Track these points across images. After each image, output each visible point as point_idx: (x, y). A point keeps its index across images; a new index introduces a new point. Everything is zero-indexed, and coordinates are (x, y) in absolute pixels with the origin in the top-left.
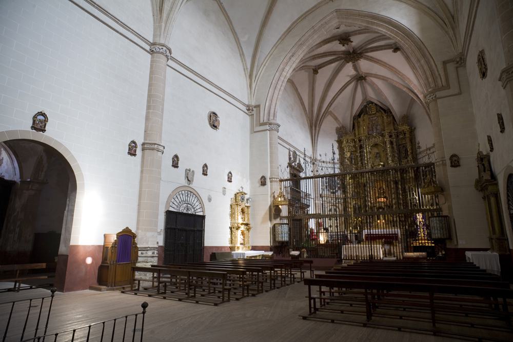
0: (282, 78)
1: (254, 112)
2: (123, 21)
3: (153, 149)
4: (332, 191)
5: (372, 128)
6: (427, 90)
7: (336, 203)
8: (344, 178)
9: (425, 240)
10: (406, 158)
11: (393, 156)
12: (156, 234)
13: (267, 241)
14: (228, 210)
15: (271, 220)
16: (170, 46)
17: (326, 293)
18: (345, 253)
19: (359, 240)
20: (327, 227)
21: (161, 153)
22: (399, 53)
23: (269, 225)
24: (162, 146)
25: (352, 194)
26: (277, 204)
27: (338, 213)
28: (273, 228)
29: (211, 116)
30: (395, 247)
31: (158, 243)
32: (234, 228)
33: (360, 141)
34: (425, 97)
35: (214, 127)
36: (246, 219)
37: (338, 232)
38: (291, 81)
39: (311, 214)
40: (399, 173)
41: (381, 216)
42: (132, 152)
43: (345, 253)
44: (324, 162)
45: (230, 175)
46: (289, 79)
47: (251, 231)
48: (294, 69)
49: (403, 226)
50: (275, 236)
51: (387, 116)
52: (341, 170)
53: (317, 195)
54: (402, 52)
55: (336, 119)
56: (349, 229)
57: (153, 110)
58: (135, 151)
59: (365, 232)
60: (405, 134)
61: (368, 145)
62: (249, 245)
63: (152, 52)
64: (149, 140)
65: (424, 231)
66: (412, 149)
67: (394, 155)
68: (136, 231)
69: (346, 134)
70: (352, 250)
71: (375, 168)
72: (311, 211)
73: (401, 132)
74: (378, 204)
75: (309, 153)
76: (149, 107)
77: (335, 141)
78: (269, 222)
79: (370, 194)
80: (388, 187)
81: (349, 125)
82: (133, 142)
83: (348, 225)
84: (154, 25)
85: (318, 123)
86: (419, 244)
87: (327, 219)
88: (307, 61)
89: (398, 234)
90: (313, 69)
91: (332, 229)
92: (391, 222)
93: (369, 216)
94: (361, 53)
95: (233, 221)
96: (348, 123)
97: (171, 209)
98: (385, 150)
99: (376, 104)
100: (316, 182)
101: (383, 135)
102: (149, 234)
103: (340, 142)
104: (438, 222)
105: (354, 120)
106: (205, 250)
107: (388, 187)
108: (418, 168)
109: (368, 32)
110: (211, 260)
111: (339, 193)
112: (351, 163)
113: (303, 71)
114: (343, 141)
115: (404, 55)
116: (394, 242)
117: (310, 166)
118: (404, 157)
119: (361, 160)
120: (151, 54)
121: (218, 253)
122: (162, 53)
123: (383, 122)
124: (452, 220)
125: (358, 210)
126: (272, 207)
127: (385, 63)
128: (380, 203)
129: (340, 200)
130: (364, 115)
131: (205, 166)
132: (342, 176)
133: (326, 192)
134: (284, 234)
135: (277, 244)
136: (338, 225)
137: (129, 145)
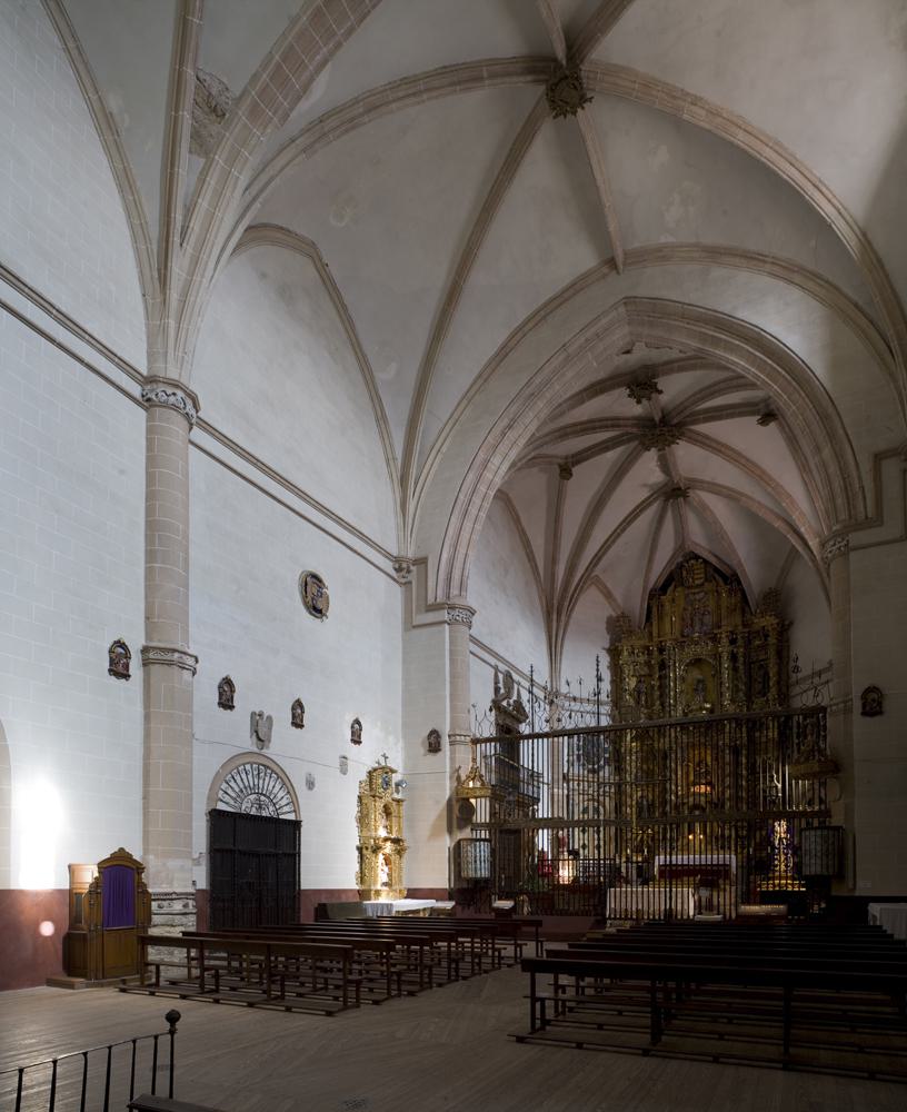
0: (482, 488)
1: (413, 577)
2: (63, 309)
3: (170, 663)
4: (590, 767)
5: (692, 620)
6: (830, 528)
7: (598, 795)
8: (620, 737)
9: (787, 878)
10: (764, 696)
11: (735, 689)
12: (190, 862)
13: (440, 878)
14: (354, 809)
15: (450, 831)
16: (194, 387)
17: (568, 989)
18: (613, 906)
19: (645, 877)
20: (576, 847)
21: (190, 673)
22: (773, 425)
23: (447, 842)
24: (191, 656)
25: (636, 776)
26: (465, 796)
27: (602, 818)
28: (454, 848)
29: (306, 584)
30: (722, 894)
31: (194, 883)
32: (367, 848)
33: (661, 651)
34: (823, 545)
35: (317, 610)
36: (395, 829)
37: (599, 859)
38: (503, 497)
39: (543, 819)
40: (744, 729)
41: (697, 825)
42: (119, 668)
43: (613, 906)
44: (575, 699)
45: (356, 726)
46: (499, 490)
47: (406, 855)
48: (513, 465)
49: (743, 848)
50: (459, 864)
51: (730, 592)
52: (613, 719)
53: (556, 777)
54: (780, 424)
55: (608, 595)
56: (624, 853)
57: (163, 562)
58: (127, 667)
59: (660, 860)
60: (766, 636)
61: (680, 661)
62: (402, 887)
63: (147, 403)
64: (159, 641)
65: (786, 859)
66: (779, 673)
67: (737, 686)
68: (143, 859)
69: (631, 632)
70: (629, 899)
71: (690, 716)
72: (543, 811)
73: (758, 632)
74: (691, 799)
75: (542, 677)
76: (150, 556)
78: (447, 837)
79: (676, 775)
80: (717, 759)
81: (637, 612)
82: (120, 644)
83: (624, 844)
84: (147, 325)
85: (566, 604)
86: (774, 886)
87: (576, 829)
88: (546, 443)
89: (730, 866)
90: (560, 466)
91: (586, 851)
92: (717, 838)
93: (671, 825)
94: (680, 425)
95: (364, 834)
96: (636, 606)
97: (221, 806)
98: (718, 673)
99: (705, 561)
100: (556, 745)
101: (715, 639)
102: (173, 864)
103: (614, 652)
104: (818, 840)
105: (649, 599)
106: (302, 898)
107: (717, 759)
108: (789, 718)
109: (703, 367)
110: (316, 920)
111: (606, 773)
112: (638, 702)
113: (535, 470)
114: (622, 650)
115: (785, 432)
116: (721, 881)
117: (542, 709)
118: (759, 693)
119: (661, 696)
120: (146, 409)
121: (333, 905)
122: (175, 407)
123: (719, 607)
124: (851, 836)
125: (646, 812)
126: (454, 802)
127: (739, 454)
128: (697, 797)
129: (607, 789)
130: (675, 587)
131: (298, 705)
132: (615, 733)
133: (576, 770)
134: (480, 863)
135: (465, 886)
136: (602, 843)
137: (111, 651)
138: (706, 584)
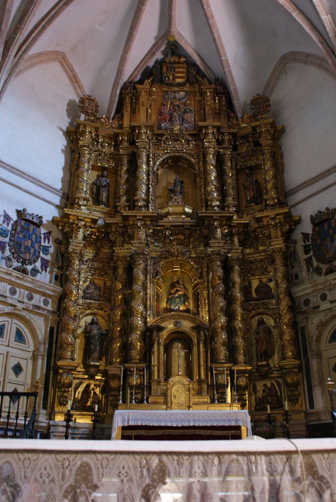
51: (216, 93)
55: (74, 79)
73: (245, 137)
77: (61, 129)
96: (106, 97)
114: (84, 132)
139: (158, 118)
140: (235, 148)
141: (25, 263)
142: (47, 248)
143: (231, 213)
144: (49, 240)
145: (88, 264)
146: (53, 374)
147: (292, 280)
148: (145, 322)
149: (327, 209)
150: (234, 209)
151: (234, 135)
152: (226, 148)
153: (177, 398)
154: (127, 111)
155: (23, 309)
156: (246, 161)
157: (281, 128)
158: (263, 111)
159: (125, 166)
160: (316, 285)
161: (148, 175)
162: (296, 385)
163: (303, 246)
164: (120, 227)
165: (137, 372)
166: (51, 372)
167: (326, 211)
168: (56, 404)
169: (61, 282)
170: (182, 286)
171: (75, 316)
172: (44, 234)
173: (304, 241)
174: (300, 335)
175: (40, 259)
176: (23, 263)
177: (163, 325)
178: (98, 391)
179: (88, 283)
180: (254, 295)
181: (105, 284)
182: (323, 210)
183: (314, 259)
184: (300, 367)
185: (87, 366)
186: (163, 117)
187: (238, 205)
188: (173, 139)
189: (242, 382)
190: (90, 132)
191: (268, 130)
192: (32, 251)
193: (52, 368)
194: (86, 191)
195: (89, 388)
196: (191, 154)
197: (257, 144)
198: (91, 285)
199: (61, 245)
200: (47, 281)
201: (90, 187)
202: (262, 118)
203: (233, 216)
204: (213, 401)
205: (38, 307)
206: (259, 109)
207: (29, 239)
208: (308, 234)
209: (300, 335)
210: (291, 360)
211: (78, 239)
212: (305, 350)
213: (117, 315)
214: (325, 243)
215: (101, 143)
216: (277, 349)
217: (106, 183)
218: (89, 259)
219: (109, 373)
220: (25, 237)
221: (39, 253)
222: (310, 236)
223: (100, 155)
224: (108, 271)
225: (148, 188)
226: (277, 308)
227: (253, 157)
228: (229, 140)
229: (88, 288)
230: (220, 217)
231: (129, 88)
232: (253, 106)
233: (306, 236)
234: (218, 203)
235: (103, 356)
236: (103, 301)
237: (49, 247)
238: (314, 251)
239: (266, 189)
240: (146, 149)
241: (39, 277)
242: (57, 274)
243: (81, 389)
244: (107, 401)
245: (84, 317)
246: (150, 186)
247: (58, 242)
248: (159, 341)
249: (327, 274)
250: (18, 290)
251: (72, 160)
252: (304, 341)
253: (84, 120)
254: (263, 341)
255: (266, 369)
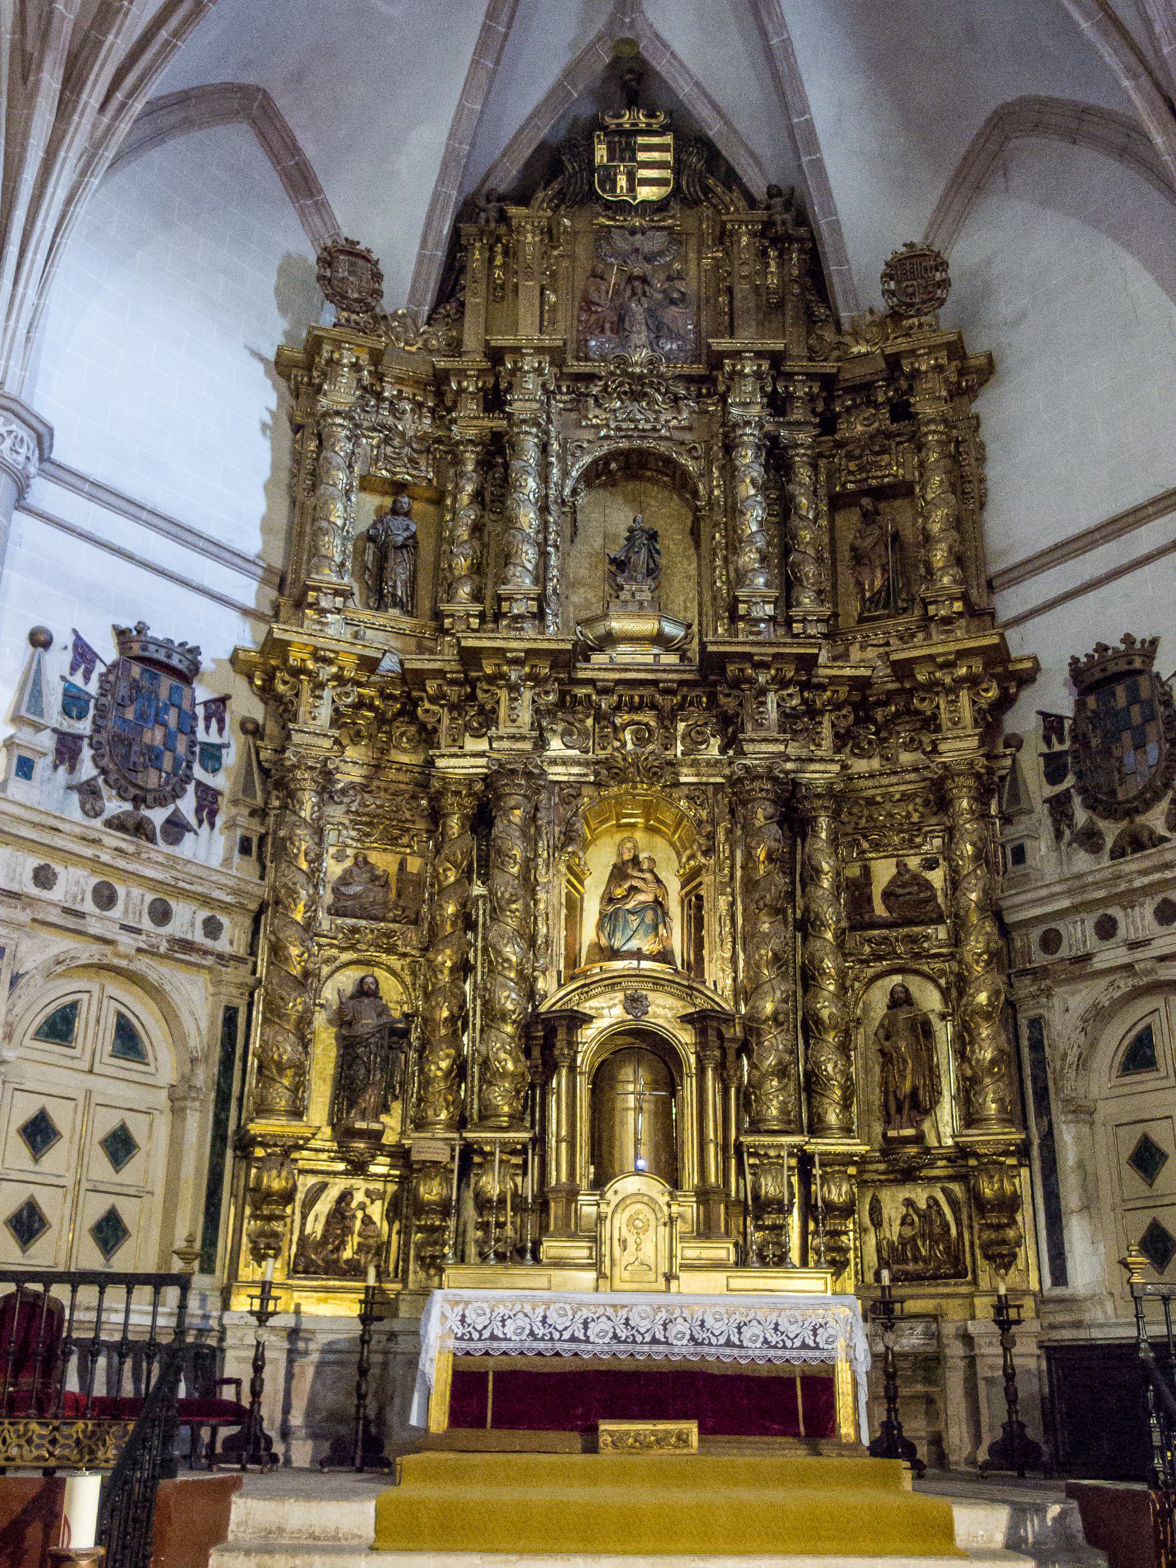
73: (864, 389)
138: (675, 208)
139: (579, 321)
140: (828, 425)
141: (144, 801)
142: (214, 751)
143: (812, 645)
144: (221, 721)
145: (346, 800)
146: (235, 1157)
147: (1005, 865)
148: (531, 994)
149: (1128, 639)
150: (822, 628)
151: (828, 382)
152: (798, 423)
153: (631, 1246)
154: (475, 295)
155: (139, 950)
156: (861, 469)
157: (983, 360)
158: (924, 302)
159: (469, 479)
160: (1084, 887)
161: (544, 510)
162: (1010, 1205)
163: (1041, 755)
164: (453, 682)
165: (505, 1157)
166: (229, 1153)
167: (1122, 647)
168: (245, 1256)
169: (261, 859)
170: (648, 876)
171: (306, 974)
172: (206, 704)
173: (1047, 740)
174: (1025, 1043)
175: (191, 788)
176: (137, 801)
177: (587, 1007)
178: (376, 1211)
179: (348, 863)
180: (880, 909)
181: (402, 865)
182: (1114, 641)
183: (1077, 801)
184: (1023, 1151)
185: (344, 1134)
186: (593, 318)
187: (835, 615)
188: (625, 393)
189: (838, 1193)
190: (356, 367)
191: (939, 368)
192: (167, 762)
193: (230, 1143)
194: (342, 565)
195: (348, 1204)
196: (682, 443)
197: (901, 411)
198: (356, 870)
199: (262, 739)
200: (215, 862)
201: (355, 546)
202: (921, 325)
203: (816, 656)
204: (742, 1262)
205: (186, 946)
206: (912, 295)
207: (157, 722)
208: (1060, 719)
209: (1025, 1043)
210: (996, 1128)
211: (318, 722)
212: (1042, 1096)
213: (441, 972)
214: (1117, 752)
215: (391, 403)
216: (949, 1085)
217: (406, 534)
218: (352, 786)
219: (415, 1157)
220: (141, 716)
221: (190, 767)
222: (1067, 724)
223: (387, 441)
224: (414, 822)
225: (544, 555)
226: (952, 955)
227: (886, 457)
228: (812, 398)
229: (345, 879)
230: (776, 656)
231: (482, 215)
232: (892, 285)
233: (1052, 724)
234: (769, 609)
235: (396, 1098)
236: (394, 921)
237: (220, 747)
238: (1080, 775)
239: (928, 565)
240: (538, 425)
241: (188, 847)
242: (248, 834)
243: (324, 1206)
244: (407, 1244)
245: (333, 973)
246: (550, 549)
247: (253, 730)
248: (574, 1060)
249: (1118, 853)
250: (121, 890)
251: (297, 458)
252: (1040, 1064)
253: (335, 325)
254: (905, 1061)
255: (912, 1150)
